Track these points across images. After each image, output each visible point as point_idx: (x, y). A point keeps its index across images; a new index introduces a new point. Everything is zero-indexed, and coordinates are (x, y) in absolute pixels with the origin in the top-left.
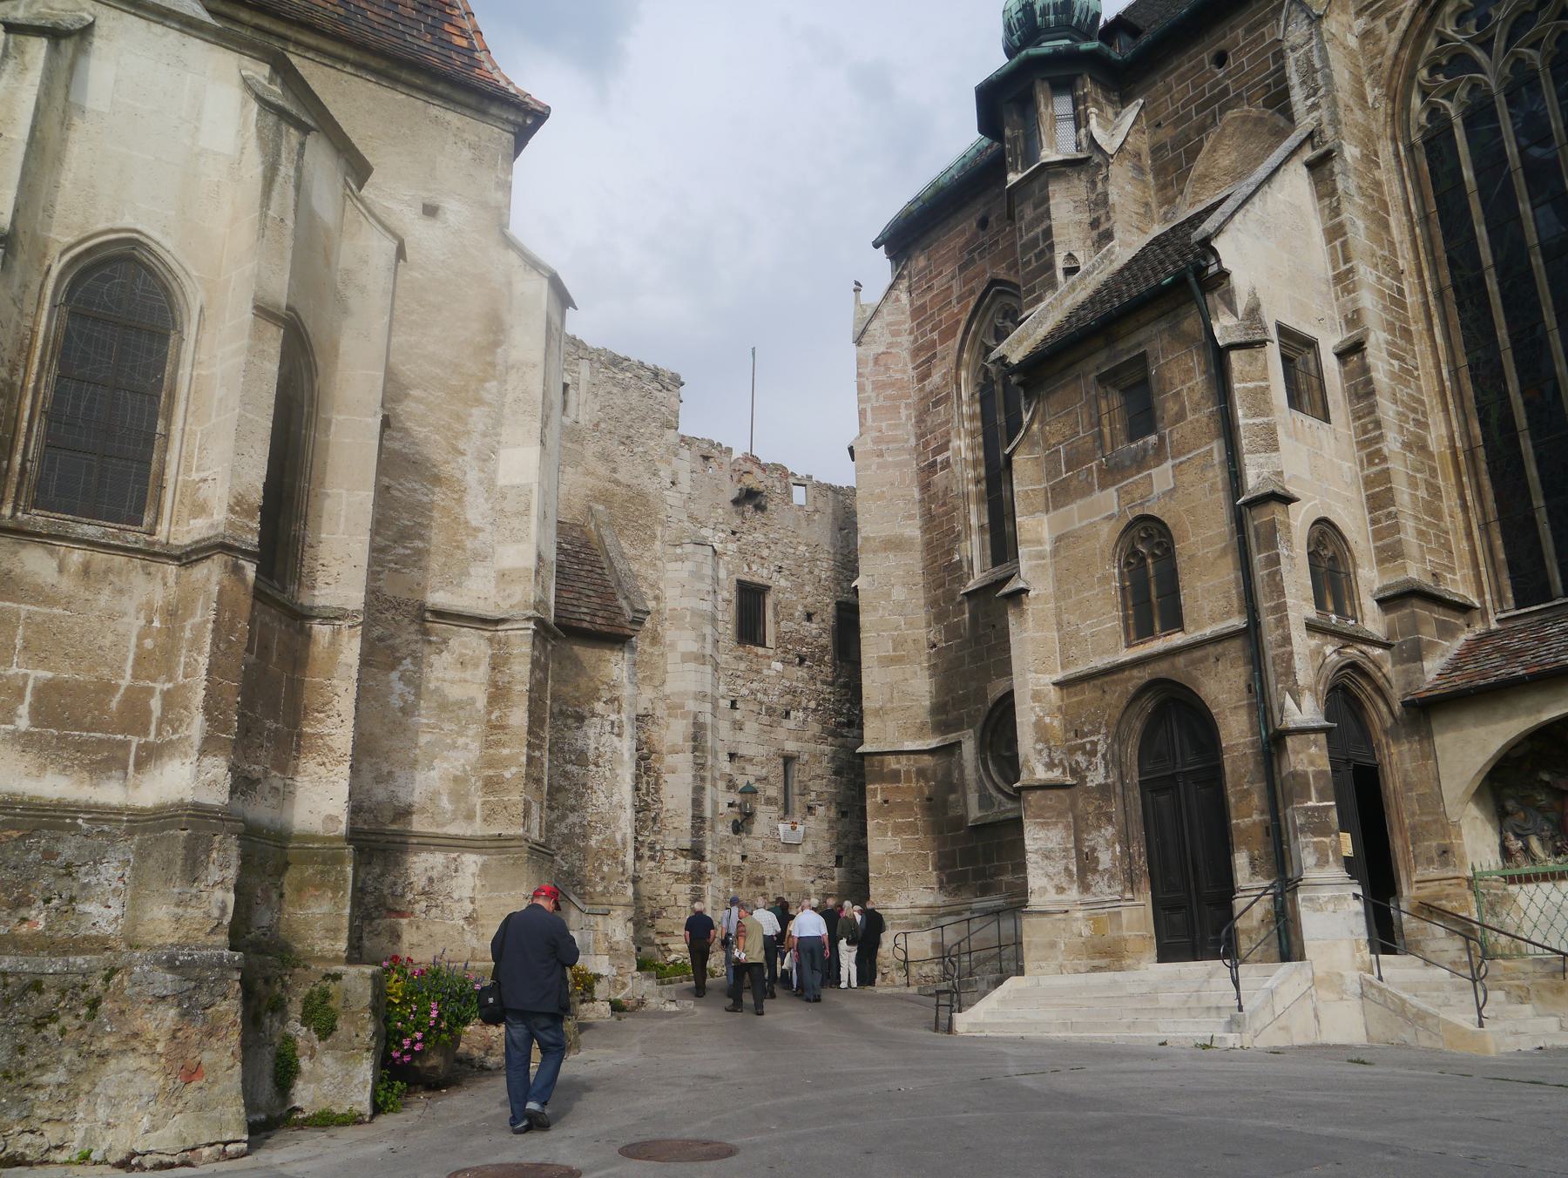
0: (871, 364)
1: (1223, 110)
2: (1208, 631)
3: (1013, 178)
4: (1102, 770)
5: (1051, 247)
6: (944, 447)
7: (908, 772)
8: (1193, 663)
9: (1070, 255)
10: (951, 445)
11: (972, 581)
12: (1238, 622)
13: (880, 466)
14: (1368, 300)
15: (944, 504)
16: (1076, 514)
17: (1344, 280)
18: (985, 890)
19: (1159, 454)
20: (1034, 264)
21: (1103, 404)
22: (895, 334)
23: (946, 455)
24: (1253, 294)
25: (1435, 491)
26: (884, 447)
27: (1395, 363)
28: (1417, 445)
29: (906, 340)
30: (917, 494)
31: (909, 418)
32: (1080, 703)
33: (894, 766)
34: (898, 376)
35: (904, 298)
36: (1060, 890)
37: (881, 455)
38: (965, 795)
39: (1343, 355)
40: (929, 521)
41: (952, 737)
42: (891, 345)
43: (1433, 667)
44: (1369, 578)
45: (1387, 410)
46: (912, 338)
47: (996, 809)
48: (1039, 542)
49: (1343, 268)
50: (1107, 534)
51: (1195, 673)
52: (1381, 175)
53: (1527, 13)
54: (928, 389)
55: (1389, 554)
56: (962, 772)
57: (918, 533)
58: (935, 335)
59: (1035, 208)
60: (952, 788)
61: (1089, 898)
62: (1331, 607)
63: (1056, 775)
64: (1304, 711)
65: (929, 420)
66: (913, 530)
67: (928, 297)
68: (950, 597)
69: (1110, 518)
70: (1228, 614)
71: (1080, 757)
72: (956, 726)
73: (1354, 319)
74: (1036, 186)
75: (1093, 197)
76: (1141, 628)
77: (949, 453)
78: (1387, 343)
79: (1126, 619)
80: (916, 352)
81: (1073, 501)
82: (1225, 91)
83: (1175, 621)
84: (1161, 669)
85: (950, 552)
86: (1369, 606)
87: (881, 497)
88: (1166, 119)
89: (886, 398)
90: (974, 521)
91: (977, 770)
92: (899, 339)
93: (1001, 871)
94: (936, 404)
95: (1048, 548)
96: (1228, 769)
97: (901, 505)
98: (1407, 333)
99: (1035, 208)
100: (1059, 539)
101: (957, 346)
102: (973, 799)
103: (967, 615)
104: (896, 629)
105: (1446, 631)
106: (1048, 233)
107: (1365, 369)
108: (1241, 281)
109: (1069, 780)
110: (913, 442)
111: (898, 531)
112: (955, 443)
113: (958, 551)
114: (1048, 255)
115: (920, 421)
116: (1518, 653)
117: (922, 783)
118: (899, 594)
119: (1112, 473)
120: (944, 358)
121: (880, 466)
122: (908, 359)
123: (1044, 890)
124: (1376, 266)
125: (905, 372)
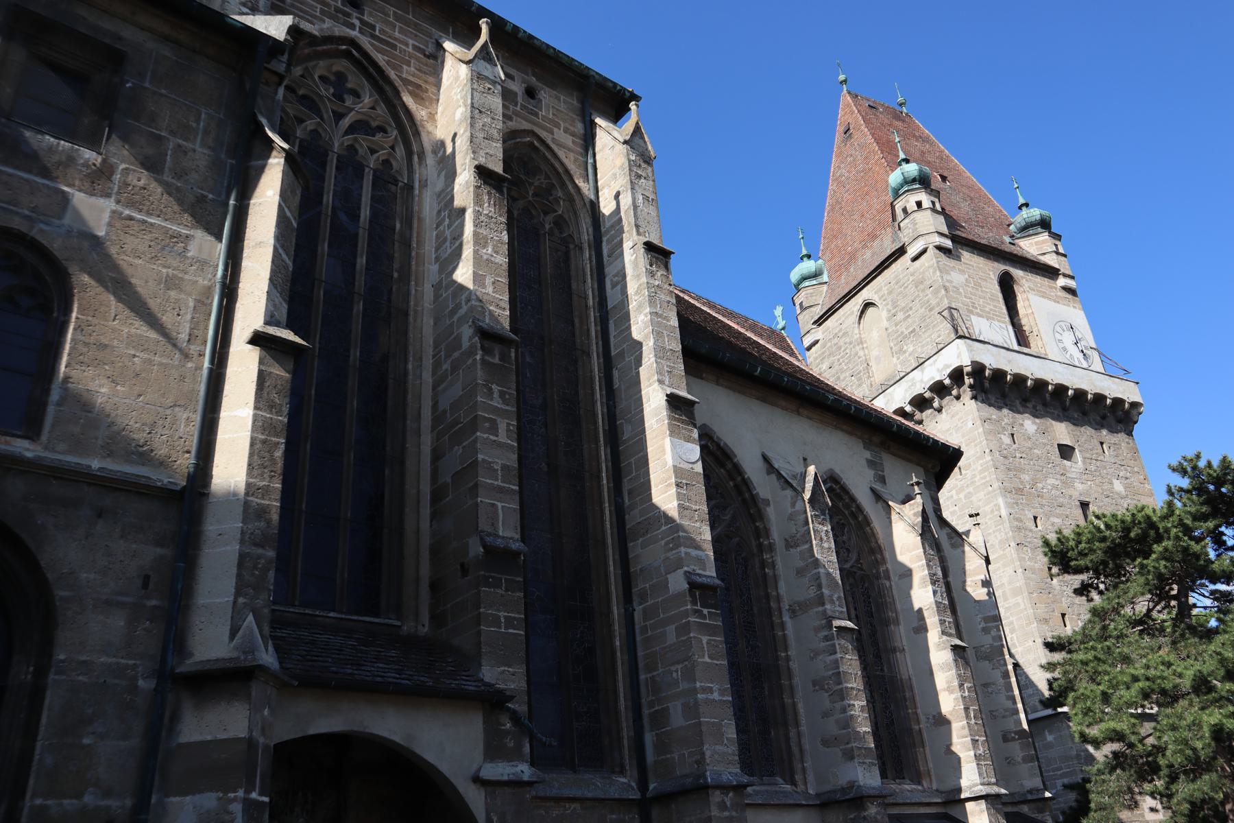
53: (367, 123)
96: (52, 700)
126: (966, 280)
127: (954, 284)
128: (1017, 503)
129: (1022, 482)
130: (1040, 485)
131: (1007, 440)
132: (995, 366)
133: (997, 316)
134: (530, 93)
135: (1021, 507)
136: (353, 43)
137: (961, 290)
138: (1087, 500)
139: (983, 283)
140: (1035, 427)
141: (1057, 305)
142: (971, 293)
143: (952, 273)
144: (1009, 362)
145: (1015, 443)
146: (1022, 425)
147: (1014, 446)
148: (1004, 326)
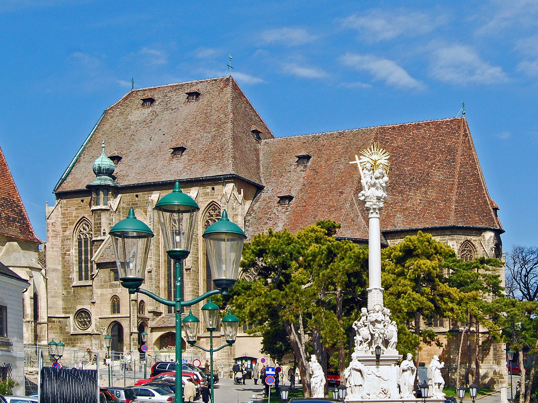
0: (51, 225)
2: (124, 316)
3: (94, 208)
4: (106, 333)
5: (101, 227)
6: (69, 250)
7: (57, 321)
8: (121, 319)
9: (104, 230)
10: (70, 251)
11: (74, 283)
12: (129, 316)
13: (53, 251)
15: (68, 264)
16: (104, 291)
18: (73, 346)
20: (97, 229)
21: (111, 273)
22: (57, 218)
23: (69, 252)
26: (53, 246)
27: (156, 273)
29: (60, 220)
30: (61, 259)
31: (60, 240)
32: (103, 322)
33: (54, 320)
34: (57, 229)
35: (59, 208)
36: (97, 350)
37: (53, 248)
38: (70, 327)
39: (149, 272)
40: (64, 266)
41: (67, 315)
46: (61, 220)
47: (77, 331)
48: (98, 294)
49: (151, 257)
50: (110, 296)
51: (121, 321)
54: (65, 235)
56: (70, 323)
57: (61, 268)
59: (98, 216)
60: (67, 326)
61: (102, 351)
62: (141, 313)
63: (98, 332)
64: (136, 330)
65: (65, 243)
66: (60, 267)
69: (110, 293)
70: (127, 314)
71: (102, 330)
72: (69, 313)
74: (99, 211)
75: (110, 218)
76: (114, 312)
77: (70, 252)
78: (155, 270)
79: (111, 310)
80: (62, 224)
81: (104, 288)
82: (137, 204)
83: (119, 312)
84: (116, 319)
87: (53, 258)
88: (125, 202)
89: (54, 234)
90: (74, 269)
91: (73, 323)
92: (58, 219)
93: (77, 343)
94: (67, 239)
95: (99, 295)
97: (57, 261)
99: (98, 216)
100: (101, 294)
101: (74, 228)
102: (72, 328)
103: (72, 290)
104: (55, 290)
106: (100, 223)
109: (100, 333)
110: (60, 246)
111: (57, 267)
112: (71, 251)
113: (71, 275)
114: (100, 228)
115: (62, 242)
116: (165, 322)
117: (60, 324)
118: (56, 282)
119: (112, 286)
120: (70, 229)
121: (53, 251)
122: (60, 225)
123: (95, 350)
124: (156, 256)
125: (59, 228)
134: (213, 189)
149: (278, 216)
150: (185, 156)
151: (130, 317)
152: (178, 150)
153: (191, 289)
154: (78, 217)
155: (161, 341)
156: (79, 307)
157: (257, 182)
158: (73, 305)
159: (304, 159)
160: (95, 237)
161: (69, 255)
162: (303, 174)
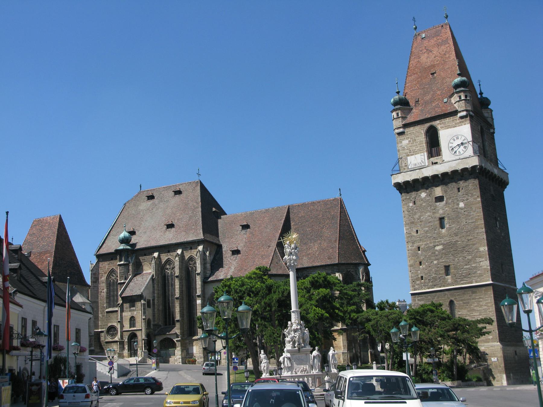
1: (145, 261)
6: (104, 290)
14: (156, 295)
17: (154, 292)
19: (135, 310)
24: (145, 297)
25: (159, 314)
28: (158, 310)
37: (94, 289)
42: (96, 272)
43: (156, 332)
44: (152, 323)
45: (156, 306)
50: (129, 317)
52: (159, 279)
55: (154, 321)
58: (103, 272)
67: (102, 266)
68: (103, 311)
73: (154, 297)
82: (145, 259)
85: (104, 305)
86: (152, 326)
98: (159, 297)
105: (158, 328)
107: (154, 303)
108: (144, 296)
119: (130, 311)
126: (409, 142)
127: (403, 147)
128: (410, 228)
129: (414, 219)
130: (422, 217)
131: (411, 204)
132: (403, 181)
133: (421, 151)
135: (411, 228)
136: (169, 258)
137: (406, 148)
138: (443, 216)
139: (417, 138)
140: (426, 194)
141: (455, 128)
142: (410, 146)
143: (403, 142)
144: (410, 176)
145: (415, 204)
146: (420, 195)
147: (414, 206)
148: (423, 154)
149: (231, 262)
150: (173, 229)
151: (141, 330)
152: (170, 226)
153: (179, 310)
154: (109, 269)
155: (161, 343)
156: (110, 324)
157: (217, 242)
158: (106, 323)
159: (246, 227)
160: (120, 281)
161: (104, 292)
162: (245, 236)
